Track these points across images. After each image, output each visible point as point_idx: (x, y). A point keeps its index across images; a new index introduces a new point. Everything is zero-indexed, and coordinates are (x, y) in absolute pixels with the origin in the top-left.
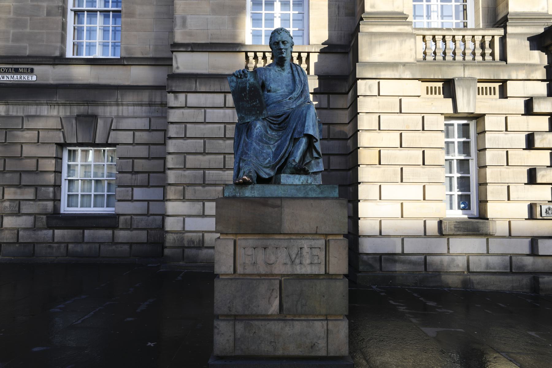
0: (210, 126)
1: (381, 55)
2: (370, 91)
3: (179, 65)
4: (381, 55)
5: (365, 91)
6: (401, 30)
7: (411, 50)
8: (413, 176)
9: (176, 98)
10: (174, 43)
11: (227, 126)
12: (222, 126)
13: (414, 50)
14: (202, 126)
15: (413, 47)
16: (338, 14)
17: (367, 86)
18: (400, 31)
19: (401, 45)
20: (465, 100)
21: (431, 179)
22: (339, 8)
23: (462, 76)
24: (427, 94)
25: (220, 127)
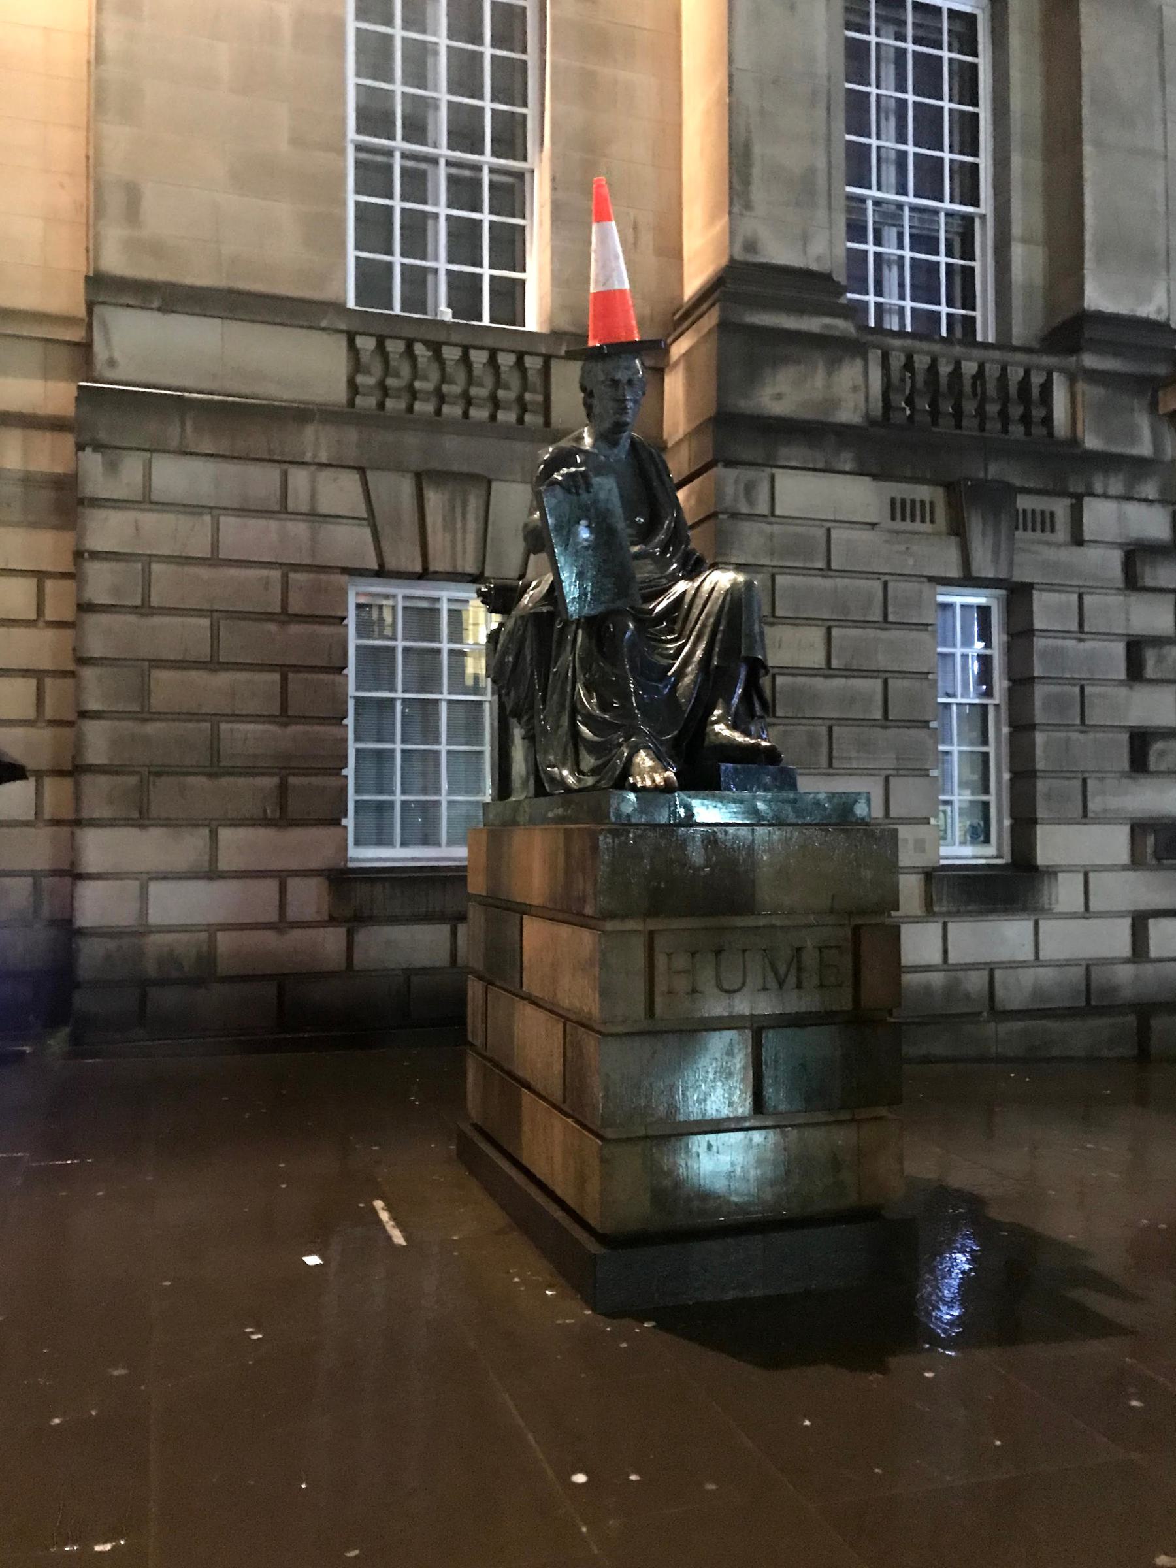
0: (233, 572)
1: (779, 397)
2: (751, 502)
3: (117, 355)
4: (779, 397)
5: (736, 500)
6: (827, 326)
7: (855, 389)
8: (858, 752)
9: (112, 467)
10: (95, 274)
11: (292, 575)
12: (276, 574)
13: (863, 390)
14: (204, 573)
15: (860, 380)
16: (635, 244)
17: (742, 486)
18: (826, 332)
19: (830, 373)
20: (989, 542)
21: (903, 759)
22: (635, 228)
23: (981, 475)
24: (893, 518)
25: (268, 577)
